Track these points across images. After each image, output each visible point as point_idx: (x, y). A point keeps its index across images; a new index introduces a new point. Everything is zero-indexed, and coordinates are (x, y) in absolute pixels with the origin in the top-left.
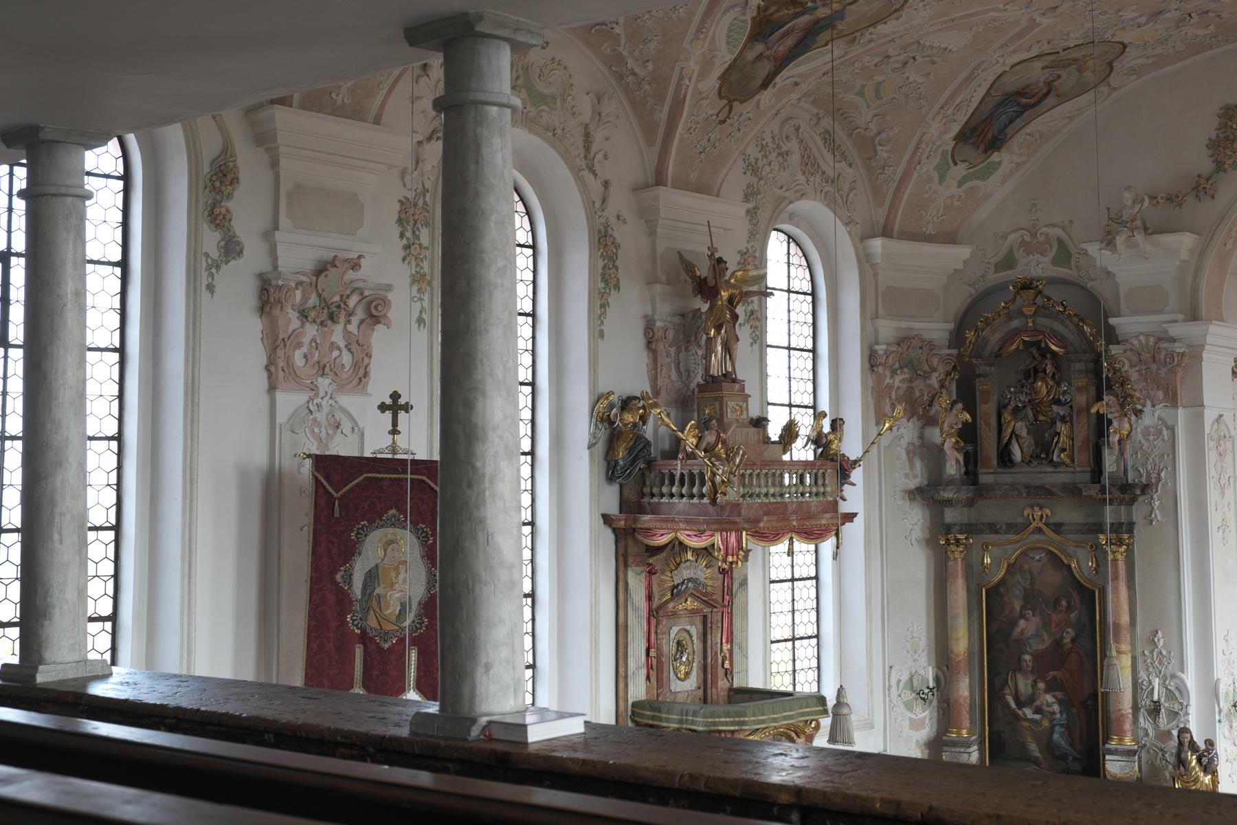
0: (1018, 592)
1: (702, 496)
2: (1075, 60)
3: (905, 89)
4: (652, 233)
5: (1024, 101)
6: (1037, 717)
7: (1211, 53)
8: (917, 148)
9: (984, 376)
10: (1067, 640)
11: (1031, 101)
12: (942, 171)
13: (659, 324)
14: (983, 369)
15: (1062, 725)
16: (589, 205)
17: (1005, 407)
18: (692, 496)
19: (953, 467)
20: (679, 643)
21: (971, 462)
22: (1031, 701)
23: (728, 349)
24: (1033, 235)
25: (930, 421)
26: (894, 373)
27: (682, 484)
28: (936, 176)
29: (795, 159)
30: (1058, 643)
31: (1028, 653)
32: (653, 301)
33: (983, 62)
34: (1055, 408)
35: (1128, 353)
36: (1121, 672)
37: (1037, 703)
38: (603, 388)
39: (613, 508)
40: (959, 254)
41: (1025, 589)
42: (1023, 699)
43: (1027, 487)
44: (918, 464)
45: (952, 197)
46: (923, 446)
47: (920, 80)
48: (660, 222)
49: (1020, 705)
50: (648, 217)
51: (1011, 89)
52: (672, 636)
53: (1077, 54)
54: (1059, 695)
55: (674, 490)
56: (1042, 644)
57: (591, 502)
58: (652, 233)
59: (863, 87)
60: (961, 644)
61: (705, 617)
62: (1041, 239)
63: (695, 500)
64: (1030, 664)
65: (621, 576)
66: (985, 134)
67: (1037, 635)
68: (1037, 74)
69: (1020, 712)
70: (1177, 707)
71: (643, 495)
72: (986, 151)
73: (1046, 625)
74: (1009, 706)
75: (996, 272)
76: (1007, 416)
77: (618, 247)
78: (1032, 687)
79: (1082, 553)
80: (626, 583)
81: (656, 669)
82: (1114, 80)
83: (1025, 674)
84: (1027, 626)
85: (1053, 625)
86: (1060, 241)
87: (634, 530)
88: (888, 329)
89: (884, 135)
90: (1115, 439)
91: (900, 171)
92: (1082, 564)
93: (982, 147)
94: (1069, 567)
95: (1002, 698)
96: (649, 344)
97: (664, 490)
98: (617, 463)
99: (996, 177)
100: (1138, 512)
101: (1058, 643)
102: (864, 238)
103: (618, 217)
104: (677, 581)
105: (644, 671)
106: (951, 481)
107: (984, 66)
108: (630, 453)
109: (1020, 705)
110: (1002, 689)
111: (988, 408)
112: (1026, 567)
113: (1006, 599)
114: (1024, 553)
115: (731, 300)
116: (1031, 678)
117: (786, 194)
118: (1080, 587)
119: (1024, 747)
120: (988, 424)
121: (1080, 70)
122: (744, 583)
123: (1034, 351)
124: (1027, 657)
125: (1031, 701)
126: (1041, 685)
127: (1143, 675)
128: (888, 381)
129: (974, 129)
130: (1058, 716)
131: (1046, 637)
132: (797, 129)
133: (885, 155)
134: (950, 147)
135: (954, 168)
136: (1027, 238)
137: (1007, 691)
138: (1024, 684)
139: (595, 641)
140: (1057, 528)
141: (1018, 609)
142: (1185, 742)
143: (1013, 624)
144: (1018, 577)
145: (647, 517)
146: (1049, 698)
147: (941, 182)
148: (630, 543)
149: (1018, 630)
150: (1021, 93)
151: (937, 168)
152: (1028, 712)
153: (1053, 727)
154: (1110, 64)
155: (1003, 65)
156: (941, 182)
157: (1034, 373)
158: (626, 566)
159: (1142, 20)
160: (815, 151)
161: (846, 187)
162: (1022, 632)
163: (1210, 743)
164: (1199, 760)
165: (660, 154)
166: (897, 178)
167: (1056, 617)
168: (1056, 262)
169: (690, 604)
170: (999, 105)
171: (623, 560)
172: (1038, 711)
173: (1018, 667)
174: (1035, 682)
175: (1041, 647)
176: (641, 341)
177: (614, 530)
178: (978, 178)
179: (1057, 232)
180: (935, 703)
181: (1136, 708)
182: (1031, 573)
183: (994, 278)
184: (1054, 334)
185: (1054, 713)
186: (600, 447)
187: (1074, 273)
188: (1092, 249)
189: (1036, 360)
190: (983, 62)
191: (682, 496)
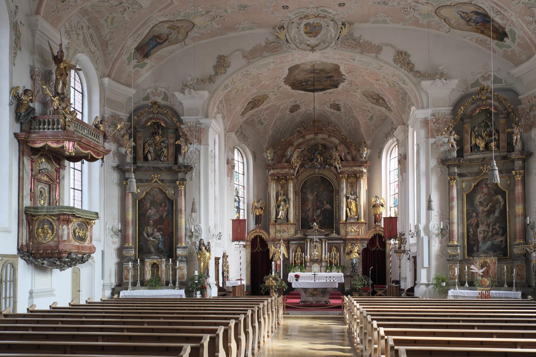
1: (58, 129)
2: (178, 27)
3: (122, 23)
4: (33, 36)
5: (159, 40)
6: (154, 240)
7: (215, 38)
8: (122, 49)
9: (140, 132)
10: (164, 216)
11: (161, 41)
12: (129, 60)
13: (36, 69)
14: (140, 129)
16: (10, 12)
17: (146, 142)
18: (53, 129)
19: (129, 159)
20: (41, 192)
21: (135, 159)
22: (152, 235)
23: (64, 84)
24: (156, 90)
25: (120, 145)
26: (110, 126)
27: (49, 125)
28: (127, 63)
29: (81, 37)
32: (33, 61)
33: (151, 17)
34: (162, 144)
35: (187, 128)
36: (182, 222)
38: (15, 85)
39: (18, 131)
40: (132, 92)
43: (153, 167)
44: (116, 159)
45: (131, 72)
46: (118, 153)
47: (128, 20)
48: (38, 31)
49: (148, 236)
50: (33, 28)
51: (156, 34)
52: (39, 188)
53: (179, 25)
54: (161, 233)
55: (45, 127)
56: (157, 217)
57: (10, 126)
58: (33, 36)
59: (108, 17)
60: (130, 216)
61: (50, 185)
62: (159, 92)
63: (55, 130)
65: (21, 159)
66: (145, 50)
67: (155, 215)
68: (164, 30)
70: (198, 234)
71: (31, 129)
72: (143, 57)
73: (158, 211)
75: (143, 101)
76: (147, 145)
77: (21, 34)
79: (169, 189)
80: (23, 162)
81: (33, 196)
82: (187, 40)
83: (150, 227)
84: (151, 212)
86: (165, 93)
87: (27, 142)
88: (108, 112)
89: (111, 41)
90: (183, 152)
91: (115, 56)
92: (170, 192)
93: (143, 55)
96: (32, 77)
97: (41, 127)
98: (21, 114)
99: (145, 69)
100: (188, 177)
101: (161, 217)
102: (101, 78)
103: (21, 23)
104: (41, 168)
105: (29, 197)
106: (128, 163)
107: (151, 19)
108: (27, 111)
109: (148, 236)
110: (143, 231)
111: (141, 142)
114: (151, 189)
115: (65, 68)
116: (152, 228)
117: (78, 48)
119: (149, 249)
120: (140, 147)
121: (178, 33)
122: (63, 177)
123: (156, 126)
124: (151, 221)
126: (156, 230)
127: (188, 226)
128: (107, 129)
129: (141, 47)
132: (82, 28)
133: (111, 49)
134: (133, 52)
135: (133, 61)
136: (154, 91)
138: (150, 230)
139: (11, 180)
140: (162, 181)
142: (201, 243)
143: (147, 211)
144: (149, 196)
145: (34, 135)
146: (158, 234)
147: (128, 65)
148: (25, 147)
149: (148, 213)
150: (158, 37)
151: (128, 59)
152: (151, 239)
153: (159, 243)
154: (187, 33)
155: (157, 21)
156: (128, 65)
157: (154, 134)
158: (23, 155)
159: (203, 13)
160: (87, 39)
161: (97, 57)
163: (209, 243)
164: (206, 248)
165: (38, 5)
166: (114, 59)
167: (161, 209)
168: (163, 99)
169: (45, 178)
170: (151, 39)
171: (21, 153)
172: (154, 238)
173: (148, 225)
174: (154, 229)
175: (156, 218)
176: (29, 75)
177: (18, 141)
178: (140, 67)
179: (164, 90)
180: (120, 236)
181: (186, 236)
183: (143, 103)
184: (163, 120)
186: (13, 106)
187: (169, 103)
188: (177, 94)
189: (156, 128)
190: (151, 17)
191: (49, 129)
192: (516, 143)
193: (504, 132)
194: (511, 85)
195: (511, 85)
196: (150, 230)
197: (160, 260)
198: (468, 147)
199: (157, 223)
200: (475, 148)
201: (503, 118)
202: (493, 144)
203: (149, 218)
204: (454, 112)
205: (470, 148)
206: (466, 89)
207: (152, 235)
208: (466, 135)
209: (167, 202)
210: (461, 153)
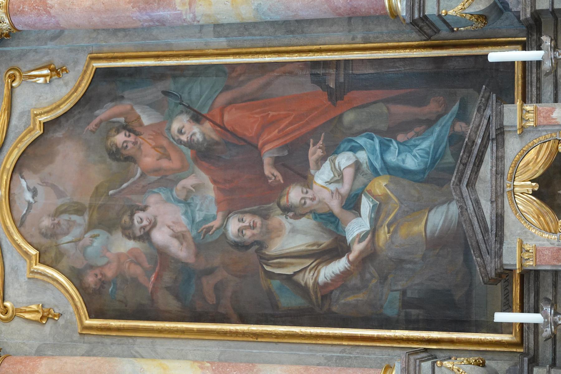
0: (97, 242)
6: (366, 205)
10: (196, 132)
15: (385, 148)
30: (204, 154)
31: (224, 226)
37: (335, 205)
41: (91, 226)
42: (325, 241)
49: (338, 248)
54: (315, 152)
64: (248, 220)
67: (186, 201)
69: (357, 248)
73: (166, 180)
74: (345, 275)
78: (297, 216)
83: (270, 233)
84: (168, 222)
85: (165, 163)
94: (46, 125)
95: (326, 292)
101: (204, 154)
112: (46, 222)
113: (110, 273)
114: (20, 224)
116: (279, 219)
118: (88, 101)
119: (439, 243)
125: (329, 220)
126: (295, 195)
130: (362, 156)
131: (188, 182)
137: (308, 279)
138: (294, 237)
141: (131, 244)
143: (162, 256)
146: (322, 176)
152: (356, 228)
153: (397, 172)
162: (179, 237)
167: (149, 159)
172: (352, 204)
173: (254, 249)
174: (287, 210)
182: (58, 213)
185: (357, 166)
196: (294, 237)
197: (513, 146)
199: (251, 192)
203: (206, 241)
207: (329, 220)
209: (105, 112)
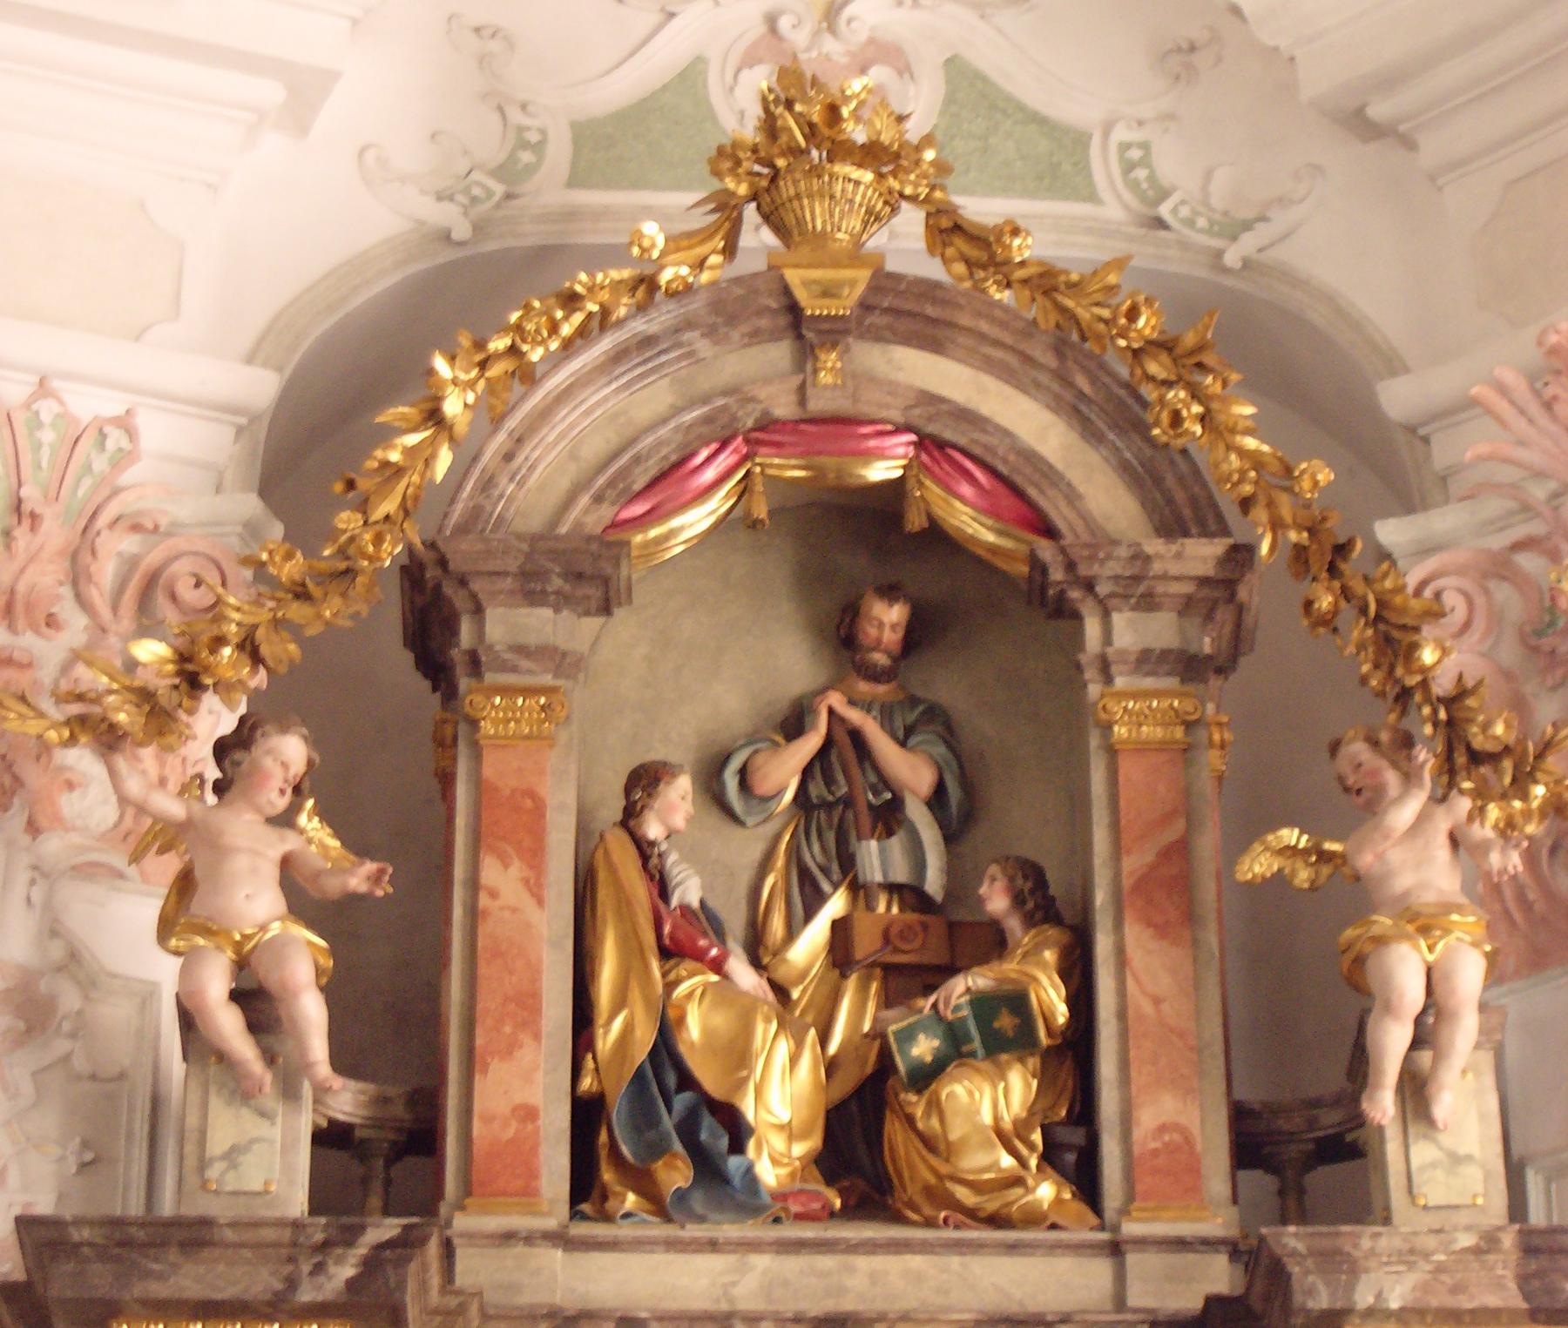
192: (1416, 1090)
193: (1170, 890)
194: (1235, 229)
195: (1235, 229)
198: (518, 1092)
200: (650, 1135)
201: (1147, 661)
202: (989, 1103)
204: (312, 443)
205: (557, 1120)
206: (502, 172)
208: (502, 879)
210: (391, 1158)
